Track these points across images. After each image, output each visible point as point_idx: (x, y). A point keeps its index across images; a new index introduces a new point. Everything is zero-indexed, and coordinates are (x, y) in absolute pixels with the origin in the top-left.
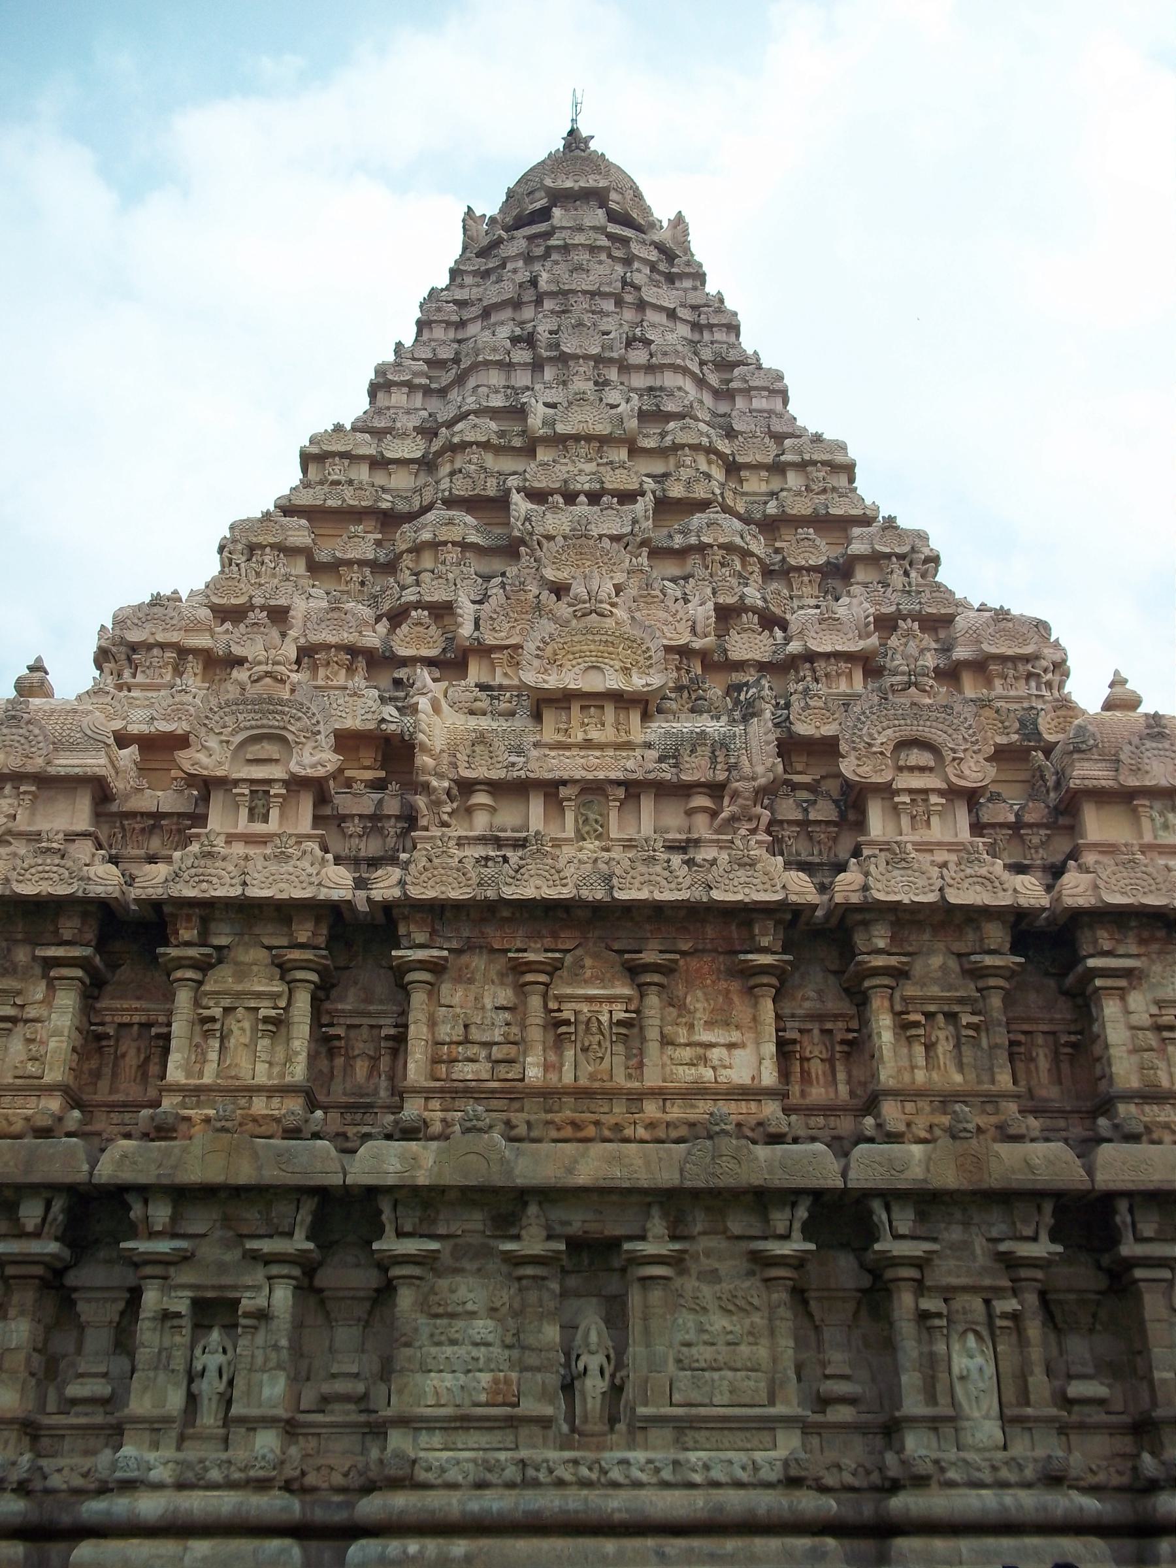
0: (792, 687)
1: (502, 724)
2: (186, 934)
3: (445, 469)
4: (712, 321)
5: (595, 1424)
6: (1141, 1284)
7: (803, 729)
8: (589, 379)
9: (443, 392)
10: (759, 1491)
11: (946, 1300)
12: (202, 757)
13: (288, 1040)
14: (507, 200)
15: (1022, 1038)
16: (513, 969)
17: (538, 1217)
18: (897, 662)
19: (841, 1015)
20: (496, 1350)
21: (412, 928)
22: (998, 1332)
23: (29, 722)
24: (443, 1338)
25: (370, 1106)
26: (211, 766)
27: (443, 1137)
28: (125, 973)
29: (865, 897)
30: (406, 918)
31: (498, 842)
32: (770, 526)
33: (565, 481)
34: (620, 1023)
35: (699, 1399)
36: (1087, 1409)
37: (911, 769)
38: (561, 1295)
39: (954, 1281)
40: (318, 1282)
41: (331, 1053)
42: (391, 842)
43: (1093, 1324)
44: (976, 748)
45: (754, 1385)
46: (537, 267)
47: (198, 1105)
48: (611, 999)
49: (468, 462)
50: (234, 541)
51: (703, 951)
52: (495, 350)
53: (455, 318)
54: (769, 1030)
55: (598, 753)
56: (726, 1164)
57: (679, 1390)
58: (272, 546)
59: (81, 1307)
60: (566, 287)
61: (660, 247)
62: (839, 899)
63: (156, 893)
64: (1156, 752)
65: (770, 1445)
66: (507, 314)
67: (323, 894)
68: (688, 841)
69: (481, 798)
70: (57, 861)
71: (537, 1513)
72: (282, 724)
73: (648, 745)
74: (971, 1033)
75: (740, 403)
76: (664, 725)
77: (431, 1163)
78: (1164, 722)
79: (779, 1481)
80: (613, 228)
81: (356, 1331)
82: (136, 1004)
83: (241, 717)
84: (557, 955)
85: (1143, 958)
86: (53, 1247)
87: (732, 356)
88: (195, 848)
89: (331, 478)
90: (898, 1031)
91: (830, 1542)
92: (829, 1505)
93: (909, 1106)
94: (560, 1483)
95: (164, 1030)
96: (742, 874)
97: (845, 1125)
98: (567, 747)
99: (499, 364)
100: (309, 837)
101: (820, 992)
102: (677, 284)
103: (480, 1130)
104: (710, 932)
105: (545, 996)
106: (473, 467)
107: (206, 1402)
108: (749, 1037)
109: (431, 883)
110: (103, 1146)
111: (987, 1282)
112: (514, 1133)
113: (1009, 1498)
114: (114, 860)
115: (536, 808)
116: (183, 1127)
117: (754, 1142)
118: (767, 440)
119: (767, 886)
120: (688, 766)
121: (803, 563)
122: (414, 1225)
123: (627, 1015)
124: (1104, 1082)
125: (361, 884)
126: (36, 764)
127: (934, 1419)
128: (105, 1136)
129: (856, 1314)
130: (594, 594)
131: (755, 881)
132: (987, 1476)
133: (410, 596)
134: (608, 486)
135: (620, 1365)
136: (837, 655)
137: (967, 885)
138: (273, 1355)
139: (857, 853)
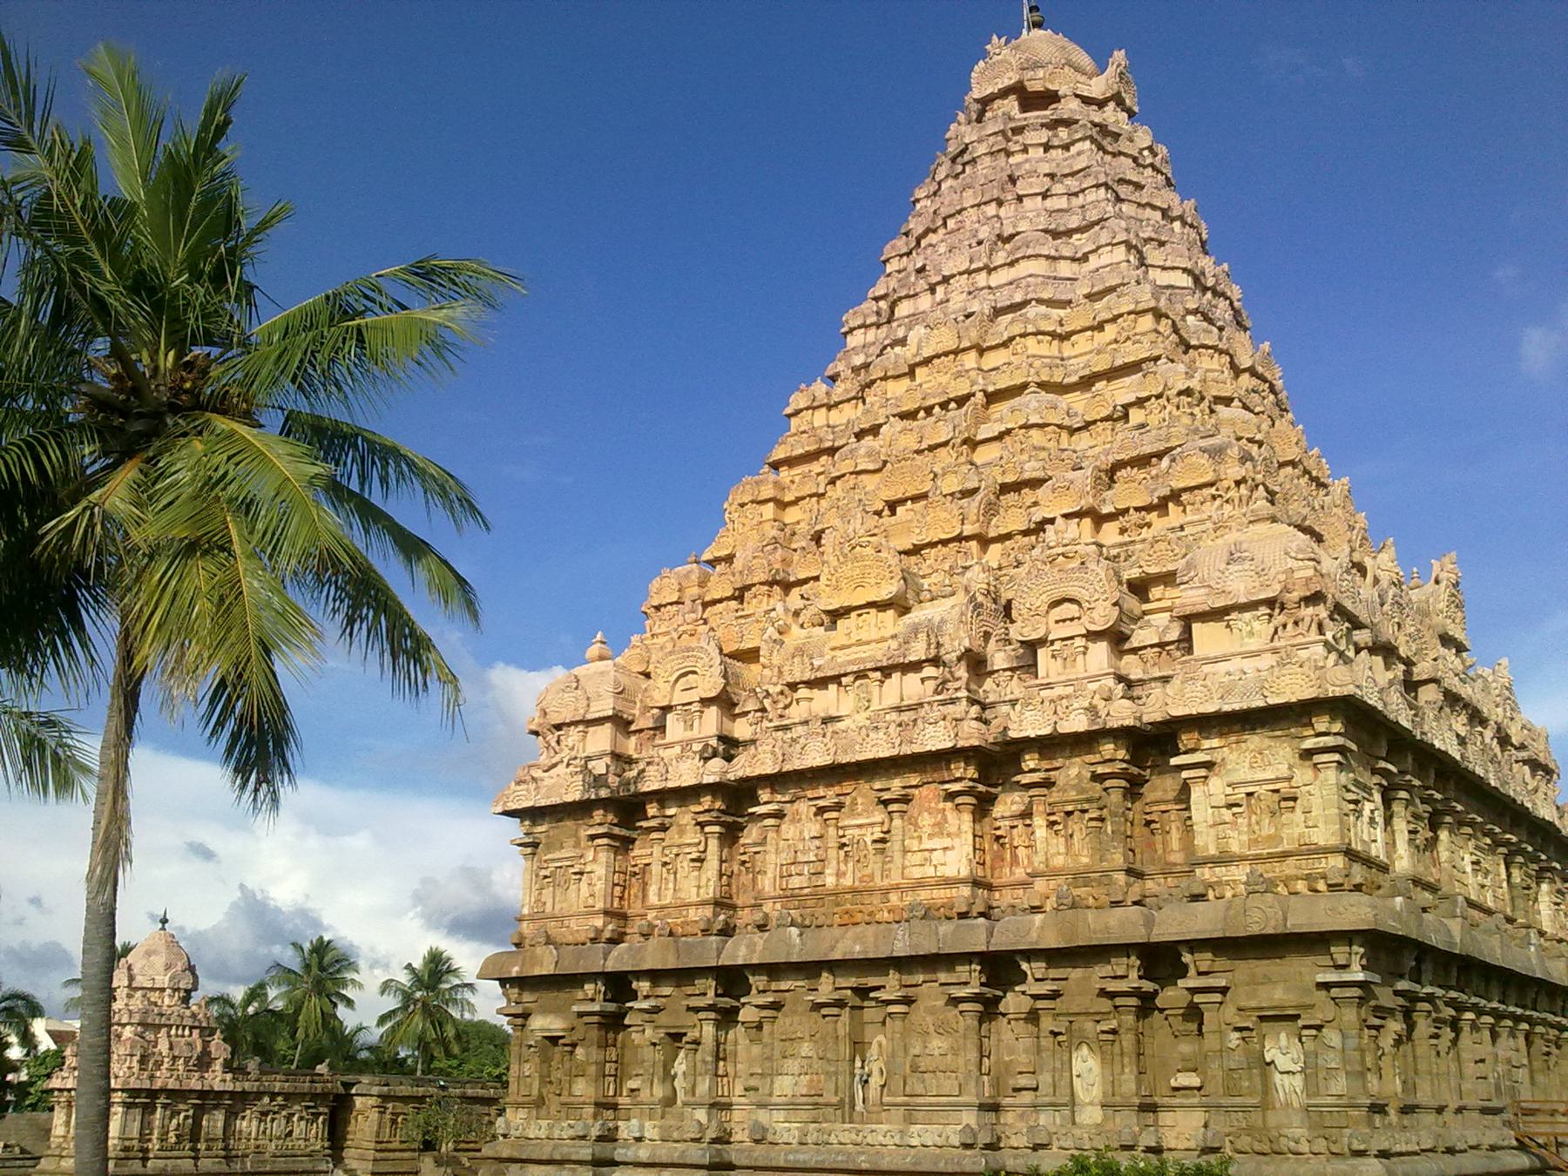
34: (875, 841)
98: (849, 647)
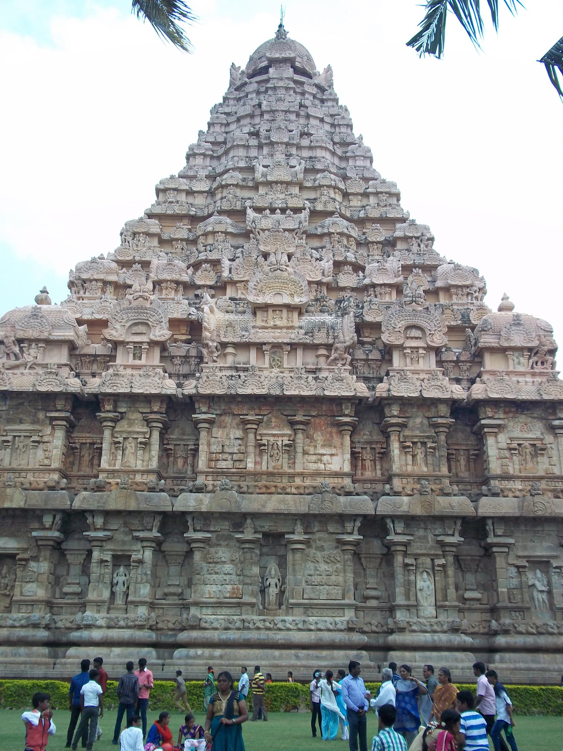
0: (366, 299)
1: (240, 317)
2: (108, 407)
3: (219, 196)
4: (341, 123)
5: (273, 606)
6: (496, 554)
7: (368, 318)
8: (283, 153)
9: (219, 158)
10: (337, 633)
11: (415, 559)
12: (113, 332)
13: (150, 451)
14: (249, 62)
15: (454, 452)
16: (242, 422)
17: (251, 524)
18: (407, 292)
19: (380, 442)
20: (234, 577)
21: (201, 405)
22: (436, 572)
23: (42, 317)
24: (212, 571)
25: (184, 478)
26: (117, 336)
27: (213, 491)
28: (83, 422)
29: (389, 394)
30: (198, 401)
31: (237, 369)
32: (361, 222)
33: (271, 203)
34: (286, 445)
35: (314, 597)
36: (472, 603)
37: (412, 338)
38: (260, 555)
39: (419, 551)
40: (162, 549)
41: (168, 456)
42: (193, 367)
43: (477, 569)
44: (439, 329)
45: (337, 592)
46: (262, 97)
47: (113, 478)
48: (283, 435)
49: (228, 193)
50: (127, 231)
51: (322, 415)
52: (241, 139)
53: (225, 122)
54: (348, 449)
55: (279, 331)
56: (327, 504)
57: (307, 593)
58: (143, 233)
59: (68, 557)
60: (274, 109)
61: (318, 86)
62: (377, 395)
63: (95, 391)
64: (516, 331)
65: (342, 615)
66: (248, 120)
67: (164, 392)
68: (316, 369)
69: (230, 350)
70: (54, 377)
71: (249, 640)
72: (147, 318)
73: (301, 328)
74: (432, 450)
75: (351, 162)
76: (308, 318)
77: (207, 502)
78: (521, 318)
79: (345, 629)
80: (297, 77)
81: (178, 568)
82: (88, 435)
83: (129, 315)
84: (260, 417)
85: (506, 420)
86: (57, 534)
87: (349, 140)
88: (111, 371)
89: (169, 200)
90: (401, 449)
91: (364, 653)
92: (365, 639)
93: (405, 481)
94: (258, 628)
95: (100, 446)
96: (337, 384)
97: (379, 487)
98: (266, 328)
99: (244, 146)
100: (158, 366)
101: (371, 432)
102: (326, 104)
103: (227, 489)
104: (324, 408)
105: (255, 434)
106: (231, 195)
107: (118, 595)
108: (339, 451)
109: (208, 387)
110: (76, 492)
111: (433, 552)
112: (241, 490)
113: (436, 637)
114: (77, 375)
115: (253, 353)
116: (108, 486)
117: (339, 495)
118: (361, 182)
119: (348, 389)
120: (317, 337)
121: (374, 240)
122: (201, 527)
123: (289, 442)
124: (486, 471)
125: (179, 385)
126: (45, 335)
127: (408, 606)
128: (76, 489)
129: (380, 564)
130: (279, 261)
131: (343, 387)
132: (428, 629)
133: (202, 257)
134: (289, 205)
135: (283, 583)
136: (385, 285)
137: (431, 389)
138: (145, 577)
139: (387, 374)
